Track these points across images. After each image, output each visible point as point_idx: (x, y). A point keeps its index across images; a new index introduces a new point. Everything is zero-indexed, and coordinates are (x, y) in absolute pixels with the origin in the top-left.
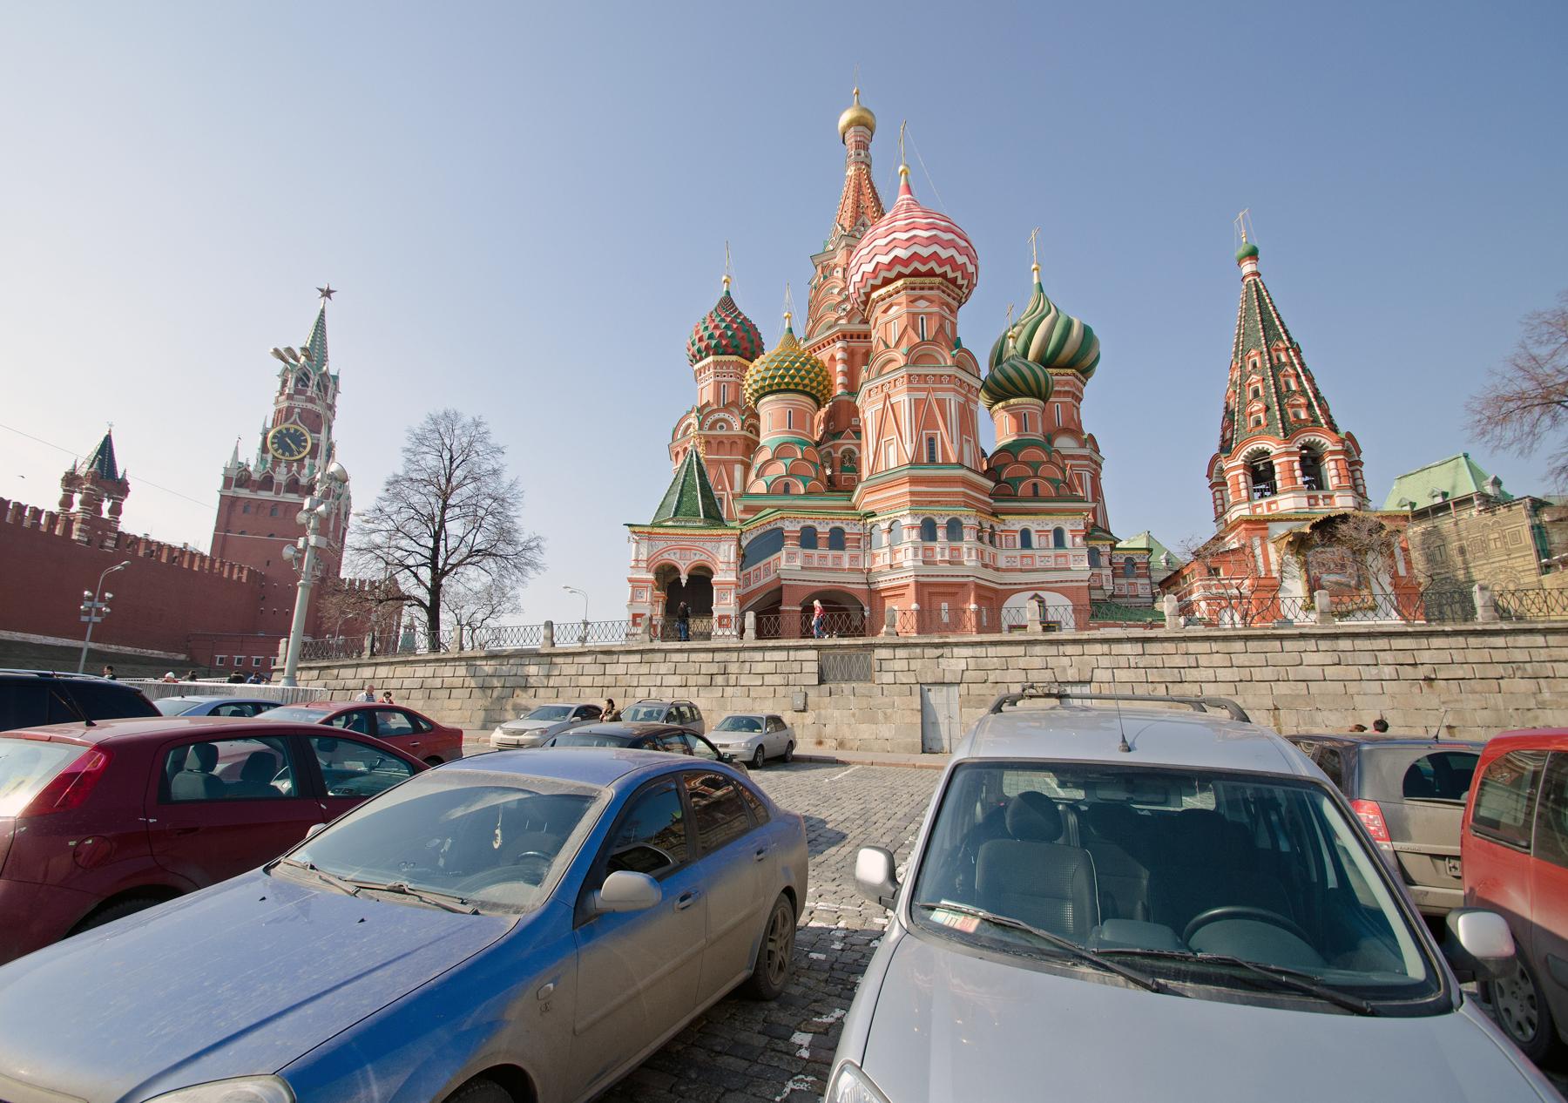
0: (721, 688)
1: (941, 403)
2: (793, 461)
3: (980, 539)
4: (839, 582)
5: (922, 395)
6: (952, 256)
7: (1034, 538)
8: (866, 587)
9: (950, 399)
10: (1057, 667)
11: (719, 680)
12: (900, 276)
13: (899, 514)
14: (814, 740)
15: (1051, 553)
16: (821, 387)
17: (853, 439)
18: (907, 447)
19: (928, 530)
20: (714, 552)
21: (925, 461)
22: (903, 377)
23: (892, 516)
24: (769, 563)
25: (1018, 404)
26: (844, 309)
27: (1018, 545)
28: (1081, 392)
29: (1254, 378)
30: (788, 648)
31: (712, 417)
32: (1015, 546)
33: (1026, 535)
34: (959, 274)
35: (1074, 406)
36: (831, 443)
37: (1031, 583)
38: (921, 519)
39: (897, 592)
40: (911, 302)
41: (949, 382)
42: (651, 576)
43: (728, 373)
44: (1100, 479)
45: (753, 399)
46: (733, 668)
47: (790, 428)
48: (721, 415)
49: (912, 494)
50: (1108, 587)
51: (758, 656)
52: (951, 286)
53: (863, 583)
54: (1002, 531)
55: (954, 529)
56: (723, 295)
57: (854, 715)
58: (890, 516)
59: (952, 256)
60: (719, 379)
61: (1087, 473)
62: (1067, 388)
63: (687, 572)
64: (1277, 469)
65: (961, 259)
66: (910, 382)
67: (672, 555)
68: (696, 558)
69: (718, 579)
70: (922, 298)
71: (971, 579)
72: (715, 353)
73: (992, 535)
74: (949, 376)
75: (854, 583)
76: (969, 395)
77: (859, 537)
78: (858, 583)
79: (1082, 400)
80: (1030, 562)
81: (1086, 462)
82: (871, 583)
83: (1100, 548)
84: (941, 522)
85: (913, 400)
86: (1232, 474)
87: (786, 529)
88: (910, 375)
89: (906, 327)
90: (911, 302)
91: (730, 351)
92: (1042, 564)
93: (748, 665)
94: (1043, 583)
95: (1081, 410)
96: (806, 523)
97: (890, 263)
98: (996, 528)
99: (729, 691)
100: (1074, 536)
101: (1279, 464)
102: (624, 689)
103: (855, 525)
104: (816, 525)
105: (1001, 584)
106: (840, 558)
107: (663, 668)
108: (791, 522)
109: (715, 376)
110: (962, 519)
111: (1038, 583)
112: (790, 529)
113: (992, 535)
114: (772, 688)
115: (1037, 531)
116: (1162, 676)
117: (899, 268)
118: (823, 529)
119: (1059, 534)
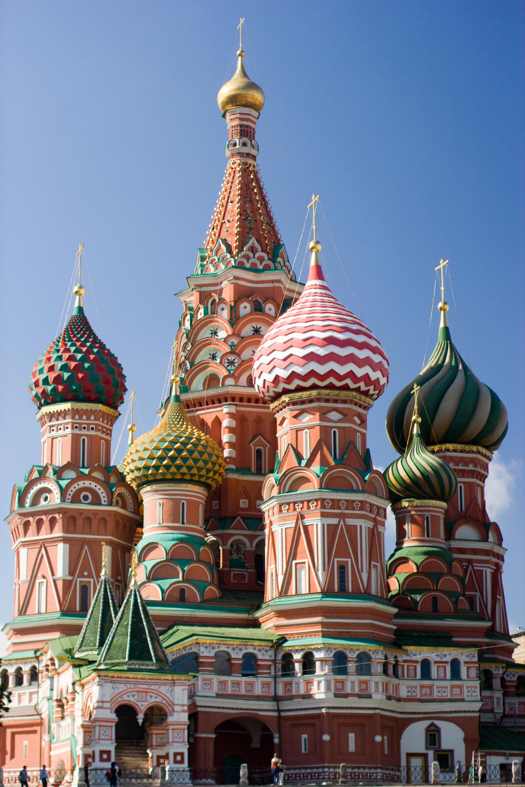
1: (352, 530)
3: (385, 672)
5: (334, 521)
6: (367, 374)
8: (275, 714)
12: (314, 387)
15: (448, 684)
16: (210, 465)
17: (244, 529)
18: (320, 573)
20: (168, 695)
27: (419, 676)
28: (486, 468)
31: (76, 485)
32: (415, 676)
33: (426, 664)
34: (372, 388)
35: (478, 485)
37: (429, 713)
38: (334, 652)
41: (361, 509)
42: (114, 716)
44: (501, 573)
48: (87, 483)
49: (323, 624)
50: (499, 710)
52: (363, 398)
53: (273, 711)
54: (405, 661)
56: (75, 313)
58: (303, 647)
60: (77, 431)
62: (471, 467)
63: (143, 712)
65: (374, 375)
66: (323, 507)
68: (153, 700)
69: (172, 720)
70: (336, 410)
71: (377, 711)
72: (74, 399)
73: (395, 667)
74: (361, 502)
75: (265, 710)
76: (379, 518)
78: (269, 710)
82: (282, 711)
83: (493, 670)
84: (352, 656)
87: (202, 655)
89: (319, 442)
92: (440, 694)
94: (439, 712)
97: (306, 375)
100: (468, 668)
104: (230, 651)
105: (401, 713)
106: (252, 684)
108: (206, 647)
109: (73, 429)
110: (371, 653)
111: (436, 713)
112: (206, 654)
113: (395, 667)
115: (436, 662)
118: (237, 655)
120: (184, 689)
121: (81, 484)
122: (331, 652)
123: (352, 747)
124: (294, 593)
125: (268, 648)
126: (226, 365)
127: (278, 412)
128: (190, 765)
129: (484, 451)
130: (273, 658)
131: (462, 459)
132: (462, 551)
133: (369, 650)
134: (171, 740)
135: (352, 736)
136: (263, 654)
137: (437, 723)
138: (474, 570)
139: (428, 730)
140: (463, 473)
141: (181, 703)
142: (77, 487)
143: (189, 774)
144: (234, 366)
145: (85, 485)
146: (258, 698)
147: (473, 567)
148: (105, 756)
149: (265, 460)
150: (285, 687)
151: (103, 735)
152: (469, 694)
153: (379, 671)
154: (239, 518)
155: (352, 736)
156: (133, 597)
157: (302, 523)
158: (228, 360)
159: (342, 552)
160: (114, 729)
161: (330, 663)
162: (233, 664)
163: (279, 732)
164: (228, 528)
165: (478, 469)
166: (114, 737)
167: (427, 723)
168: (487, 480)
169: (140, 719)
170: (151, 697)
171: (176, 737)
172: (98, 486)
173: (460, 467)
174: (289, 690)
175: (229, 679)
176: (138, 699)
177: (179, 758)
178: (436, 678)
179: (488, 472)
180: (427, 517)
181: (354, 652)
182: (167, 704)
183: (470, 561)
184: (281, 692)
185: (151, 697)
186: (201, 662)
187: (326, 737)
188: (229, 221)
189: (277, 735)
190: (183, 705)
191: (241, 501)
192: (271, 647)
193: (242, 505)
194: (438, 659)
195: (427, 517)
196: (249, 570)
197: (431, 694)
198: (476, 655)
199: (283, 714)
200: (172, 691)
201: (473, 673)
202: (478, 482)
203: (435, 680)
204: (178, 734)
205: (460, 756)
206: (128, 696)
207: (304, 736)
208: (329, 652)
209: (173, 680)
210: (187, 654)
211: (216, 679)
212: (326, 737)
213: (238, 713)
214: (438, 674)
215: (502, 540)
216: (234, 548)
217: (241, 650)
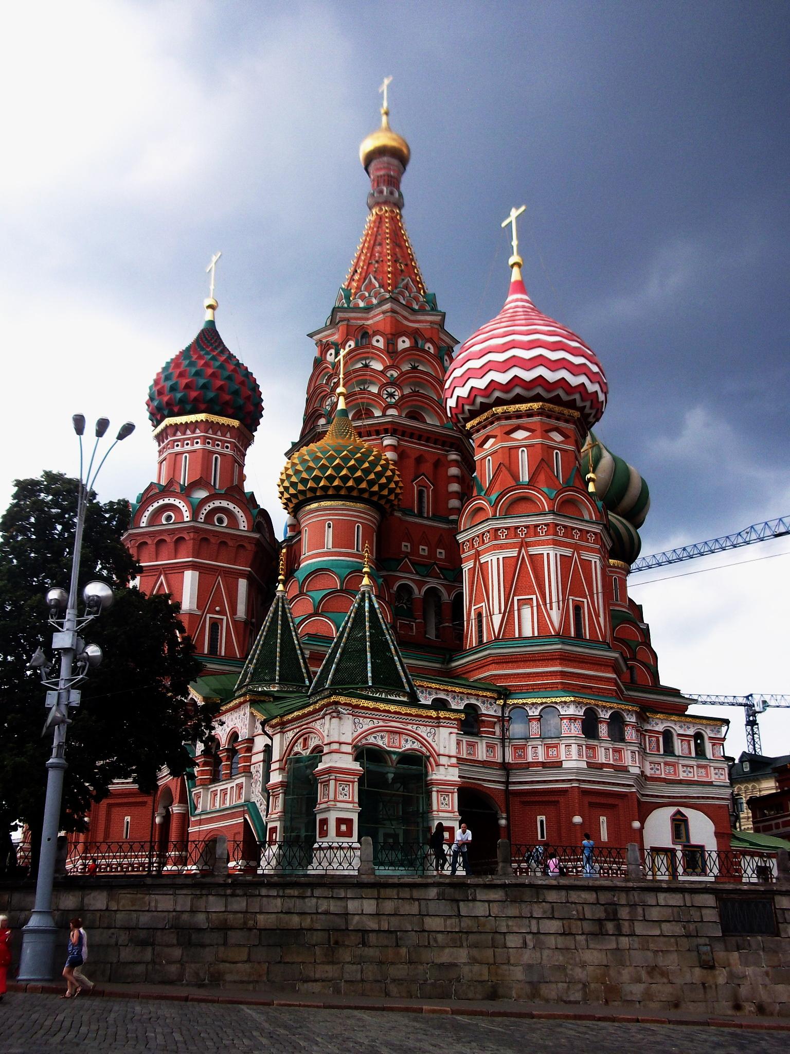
0: (614, 938)
1: (586, 564)
9: (595, 562)
11: (610, 927)
13: (558, 700)
14: (730, 1004)
15: (693, 763)
17: (413, 573)
19: (589, 727)
20: (430, 740)
21: (573, 634)
22: (546, 525)
23: (549, 701)
26: (391, 395)
27: (662, 752)
32: (659, 751)
40: (545, 431)
43: (224, 442)
46: (624, 913)
51: (650, 899)
54: (646, 731)
55: (617, 724)
57: (767, 974)
58: (544, 700)
59: (583, 384)
67: (379, 739)
68: (408, 746)
75: (489, 781)
77: (496, 720)
78: (494, 781)
85: (558, 556)
88: (557, 525)
90: (545, 431)
91: (230, 411)
92: (685, 774)
93: (640, 910)
94: (685, 797)
99: (624, 941)
102: (490, 937)
103: (491, 704)
107: (538, 912)
110: (625, 714)
114: (673, 940)
115: (679, 735)
117: (539, 390)
120: (451, 733)
124: (517, 636)
126: (385, 396)
127: (478, 431)
134: (435, 807)
135: (603, 819)
137: (686, 811)
144: (394, 398)
146: (485, 764)
148: (343, 828)
149: (428, 502)
150: (515, 752)
151: (341, 794)
155: (603, 819)
157: (527, 552)
158: (387, 391)
159: (577, 590)
163: (508, 812)
170: (407, 741)
171: (443, 804)
176: (389, 742)
185: (407, 741)
187: (577, 819)
188: (377, 262)
189: (504, 815)
190: (450, 757)
191: (404, 544)
193: (404, 549)
199: (512, 788)
200: (435, 734)
206: (375, 738)
209: (438, 718)
212: (577, 819)
214: (682, 750)
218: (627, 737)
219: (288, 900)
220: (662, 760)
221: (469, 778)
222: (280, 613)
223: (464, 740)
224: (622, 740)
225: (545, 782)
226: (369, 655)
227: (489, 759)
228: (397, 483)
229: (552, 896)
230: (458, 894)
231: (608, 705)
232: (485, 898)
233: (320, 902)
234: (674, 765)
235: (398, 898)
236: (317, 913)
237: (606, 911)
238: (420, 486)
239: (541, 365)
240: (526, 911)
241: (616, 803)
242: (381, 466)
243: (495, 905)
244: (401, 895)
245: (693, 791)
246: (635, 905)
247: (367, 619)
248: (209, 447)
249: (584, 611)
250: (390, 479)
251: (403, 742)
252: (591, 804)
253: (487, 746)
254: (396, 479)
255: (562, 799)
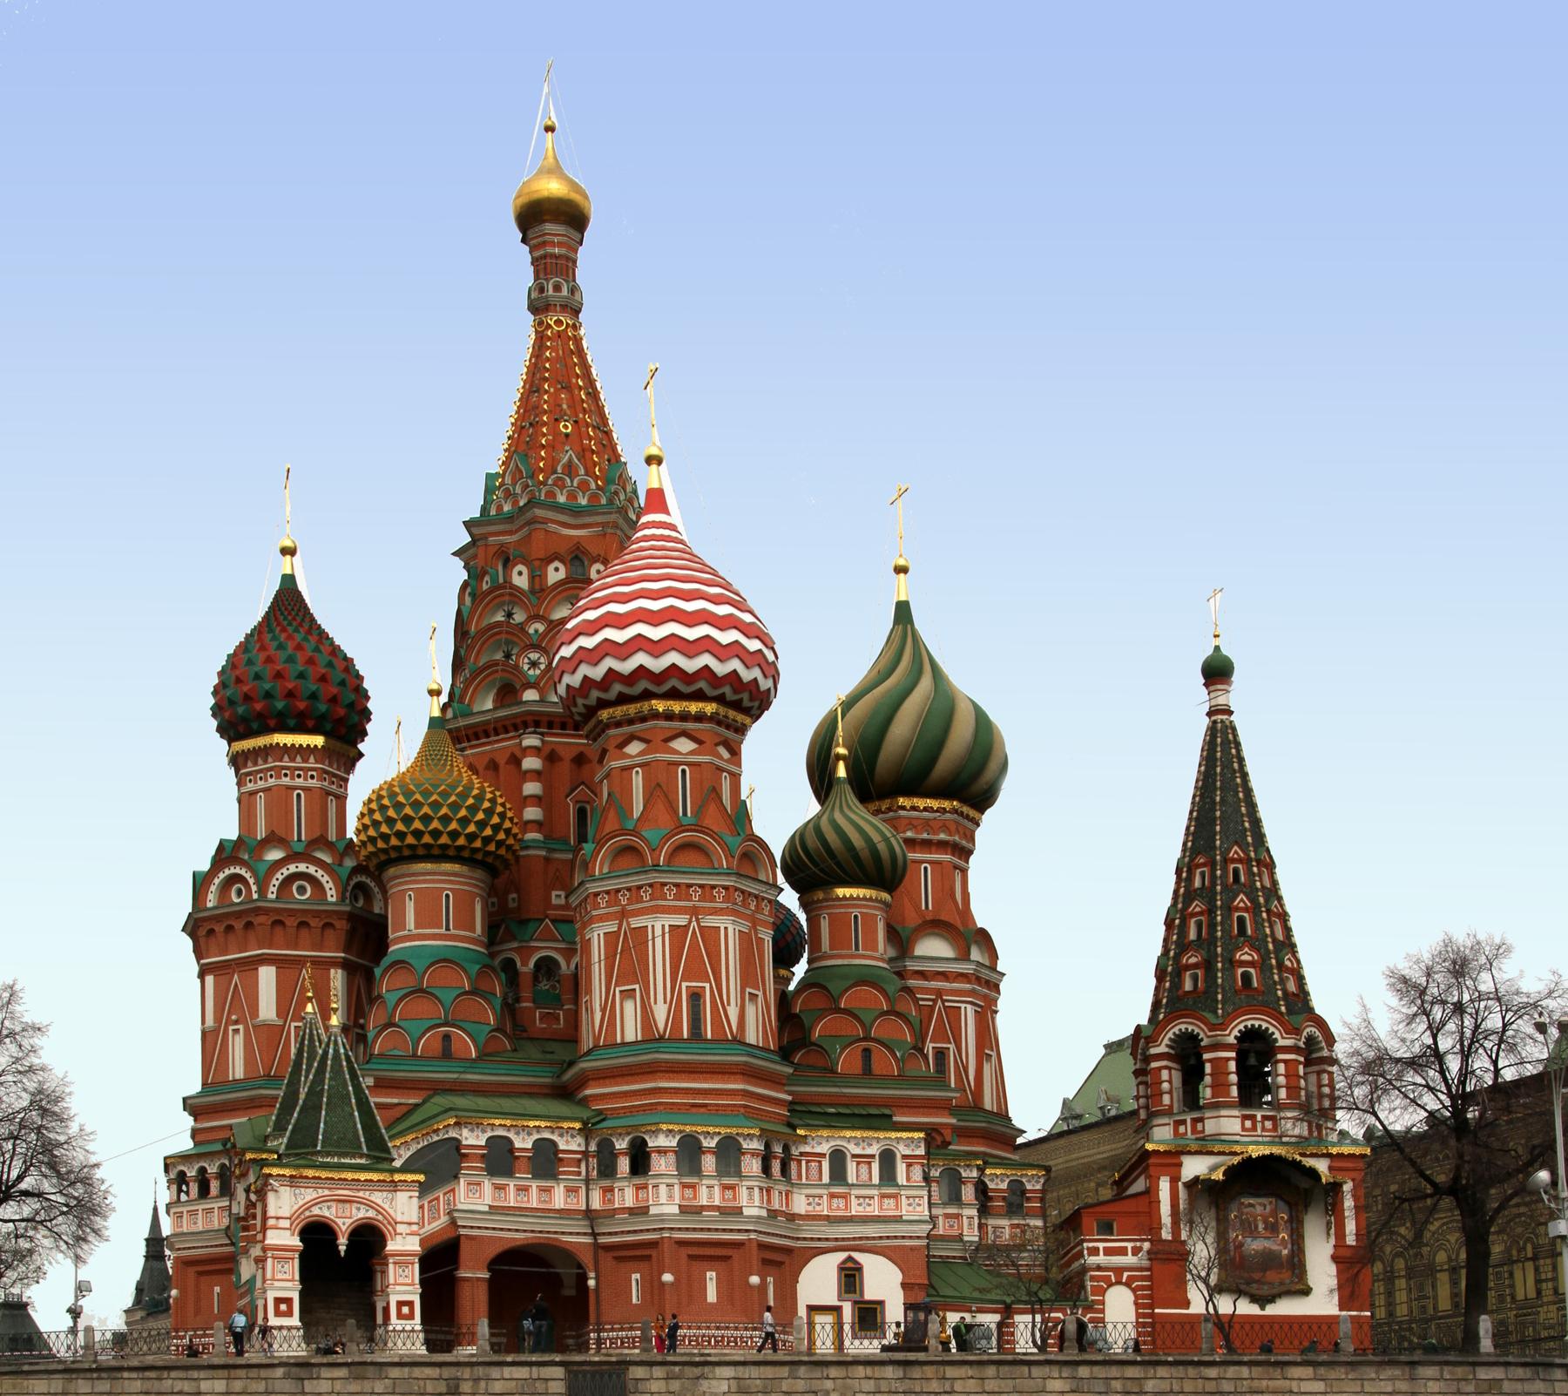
2: (458, 996)
3: (766, 1169)
4: (548, 1232)
7: (851, 1167)
8: (588, 1240)
10: (821, 1391)
15: (875, 1192)
17: (557, 941)
20: (386, 1206)
21: (685, 1036)
24: (437, 1199)
25: (851, 898)
27: (826, 1179)
28: (972, 840)
29: (1197, 906)
30: (530, 1364)
32: (821, 1179)
33: (838, 1158)
35: (956, 867)
36: (515, 945)
37: (843, 1239)
38: (678, 1137)
39: (638, 1253)
42: (296, 1242)
45: (371, 848)
47: (448, 929)
48: (302, 867)
53: (585, 1234)
54: (802, 1154)
55: (729, 1152)
61: (969, 1007)
62: (942, 836)
63: (346, 1236)
64: (1208, 1068)
68: (361, 1215)
71: (753, 1236)
75: (571, 1234)
77: (579, 1156)
78: (578, 1234)
79: (970, 852)
80: (842, 1205)
81: (968, 986)
82: (599, 1234)
83: (962, 1171)
86: (1154, 1065)
87: (464, 1143)
91: (310, 724)
92: (861, 1209)
93: (483, 1384)
94: (861, 1239)
95: (970, 873)
96: (496, 1133)
98: (795, 1152)
100: (909, 1165)
101: (1210, 1061)
104: (511, 1135)
105: (798, 1239)
106: (548, 1190)
108: (472, 1130)
110: (741, 1140)
111: (854, 1239)
115: (854, 1156)
116: (1000, 1387)
119: (887, 1158)
120: (411, 1197)
121: (292, 868)
122: (674, 1137)
123: (712, 1295)
125: (575, 1133)
128: (423, 1322)
129: (966, 809)
130: (584, 1149)
131: (927, 820)
132: (922, 975)
133: (737, 1134)
134: (391, 1280)
136: (567, 1142)
138: (945, 1007)
139: (842, 1268)
140: (927, 845)
141: (406, 1219)
142: (286, 873)
143: (421, 1336)
145: (299, 870)
147: (943, 1001)
150: (604, 1196)
152: (911, 1208)
153: (755, 1169)
154: (547, 920)
156: (332, 1046)
160: (297, 1262)
161: (672, 1157)
162: (518, 1157)
164: (531, 939)
165: (957, 838)
166: (297, 1277)
167: (843, 1256)
168: (972, 859)
169: (342, 1243)
170: (358, 1209)
172: (320, 872)
173: (925, 836)
174: (609, 1200)
175: (512, 1184)
177: (405, 1310)
178: (855, 1182)
179: (974, 845)
180: (856, 917)
181: (712, 1138)
182: (385, 1222)
183: (939, 993)
184: (596, 1204)
185: (358, 1209)
186: (465, 1155)
187: (667, 1277)
189: (592, 1275)
190: (410, 1224)
191: (554, 893)
192: (580, 1129)
193: (554, 901)
194: (858, 1151)
195: (856, 917)
196: (565, 1007)
197: (846, 1207)
198: (923, 1145)
199: (602, 1240)
200: (392, 1199)
201: (917, 1173)
202: (956, 860)
203: (853, 1185)
204: (404, 1271)
205: (895, 1312)
206: (321, 1208)
207: (636, 1276)
208: (670, 1138)
209: (393, 1181)
210: (439, 1141)
211: (487, 1185)
212: (667, 1277)
213: (527, 1239)
215: (998, 958)
216: (542, 972)
217: (529, 1134)
218: (745, 1169)
219: (147, 1382)
220: (825, 1192)
221: (540, 1232)
222: (306, 1042)
223: (534, 1186)
224: (739, 1174)
225: (635, 1232)
226: (323, 1113)
227: (568, 1207)
228: (511, 819)
229: (395, 1373)
230: (302, 1373)
231: (711, 1129)
232: (329, 1376)
233: (175, 1382)
234: (845, 1197)
235: (247, 1378)
236: (173, 1393)
237: (448, 1385)
238: (577, 802)
239: (673, 649)
240: (367, 1386)
241: (730, 1254)
242: (489, 800)
243: (339, 1381)
244: (250, 1375)
245: (871, 1230)
246: (479, 1379)
247: (329, 1068)
248: (286, 781)
249: (705, 1001)
250: (502, 816)
251: (354, 1211)
252: (691, 1257)
253: (568, 1191)
254: (509, 814)
255: (654, 1253)
